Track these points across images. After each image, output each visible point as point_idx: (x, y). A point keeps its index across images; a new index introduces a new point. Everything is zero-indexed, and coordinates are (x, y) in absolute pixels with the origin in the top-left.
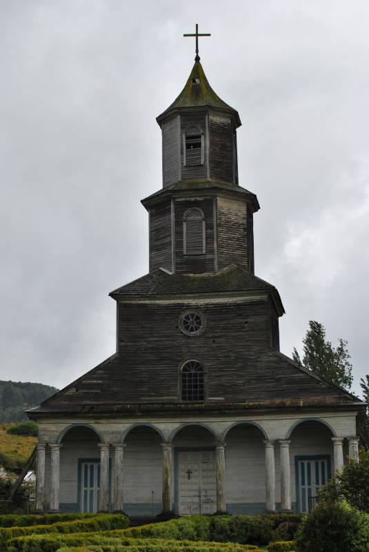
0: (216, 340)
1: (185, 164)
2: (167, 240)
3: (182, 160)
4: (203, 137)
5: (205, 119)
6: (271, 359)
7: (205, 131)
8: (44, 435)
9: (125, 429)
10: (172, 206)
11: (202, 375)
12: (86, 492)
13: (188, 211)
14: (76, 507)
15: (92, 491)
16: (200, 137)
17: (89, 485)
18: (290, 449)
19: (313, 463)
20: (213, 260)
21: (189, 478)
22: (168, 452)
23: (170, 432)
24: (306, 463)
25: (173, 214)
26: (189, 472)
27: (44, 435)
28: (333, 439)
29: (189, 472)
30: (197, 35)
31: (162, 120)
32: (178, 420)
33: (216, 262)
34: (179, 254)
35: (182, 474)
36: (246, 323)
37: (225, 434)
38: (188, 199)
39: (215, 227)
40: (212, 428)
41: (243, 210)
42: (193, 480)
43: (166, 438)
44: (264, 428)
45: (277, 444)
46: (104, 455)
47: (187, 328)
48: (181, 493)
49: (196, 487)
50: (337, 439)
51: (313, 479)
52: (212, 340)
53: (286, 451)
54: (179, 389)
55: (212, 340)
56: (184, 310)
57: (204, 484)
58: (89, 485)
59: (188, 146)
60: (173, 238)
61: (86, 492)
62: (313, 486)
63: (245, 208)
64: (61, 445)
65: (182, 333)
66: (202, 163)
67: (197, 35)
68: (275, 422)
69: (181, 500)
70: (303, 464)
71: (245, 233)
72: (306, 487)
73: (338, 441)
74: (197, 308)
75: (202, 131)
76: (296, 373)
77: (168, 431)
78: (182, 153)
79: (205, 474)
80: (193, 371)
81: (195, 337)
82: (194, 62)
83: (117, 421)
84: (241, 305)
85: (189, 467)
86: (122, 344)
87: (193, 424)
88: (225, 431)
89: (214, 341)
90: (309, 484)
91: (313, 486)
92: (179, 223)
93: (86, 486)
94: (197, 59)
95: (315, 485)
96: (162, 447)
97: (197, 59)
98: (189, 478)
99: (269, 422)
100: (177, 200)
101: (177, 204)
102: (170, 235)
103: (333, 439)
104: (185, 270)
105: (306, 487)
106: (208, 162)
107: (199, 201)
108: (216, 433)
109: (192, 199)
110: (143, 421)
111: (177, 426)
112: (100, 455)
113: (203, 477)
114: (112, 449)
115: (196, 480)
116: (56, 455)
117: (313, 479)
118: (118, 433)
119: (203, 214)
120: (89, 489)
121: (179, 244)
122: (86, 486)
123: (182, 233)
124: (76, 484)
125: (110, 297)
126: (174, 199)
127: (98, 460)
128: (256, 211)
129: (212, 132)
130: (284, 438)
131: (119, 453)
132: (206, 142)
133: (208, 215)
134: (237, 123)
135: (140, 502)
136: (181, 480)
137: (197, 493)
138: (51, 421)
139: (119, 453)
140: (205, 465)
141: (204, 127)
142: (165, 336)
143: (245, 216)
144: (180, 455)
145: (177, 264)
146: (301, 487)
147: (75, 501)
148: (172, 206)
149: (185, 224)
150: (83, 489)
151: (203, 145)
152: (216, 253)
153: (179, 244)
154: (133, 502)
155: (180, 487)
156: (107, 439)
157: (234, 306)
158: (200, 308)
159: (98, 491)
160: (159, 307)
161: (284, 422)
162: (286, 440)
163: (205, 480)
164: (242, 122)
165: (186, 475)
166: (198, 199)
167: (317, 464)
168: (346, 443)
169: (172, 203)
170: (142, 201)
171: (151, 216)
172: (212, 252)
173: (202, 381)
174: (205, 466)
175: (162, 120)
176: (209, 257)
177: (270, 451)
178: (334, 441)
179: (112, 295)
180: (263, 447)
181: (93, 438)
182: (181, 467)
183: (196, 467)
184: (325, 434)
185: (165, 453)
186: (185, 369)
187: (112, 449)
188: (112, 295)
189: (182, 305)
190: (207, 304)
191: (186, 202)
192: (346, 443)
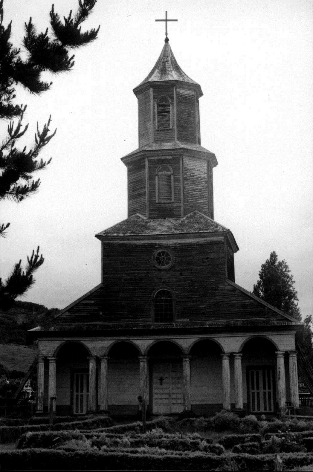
0: (182, 272)
1: (157, 129)
2: (142, 191)
3: (155, 125)
4: (171, 106)
5: (173, 91)
6: (226, 288)
7: (173, 101)
8: (43, 350)
9: (109, 345)
10: (147, 163)
11: (171, 301)
12: (77, 396)
13: (160, 167)
14: (70, 408)
15: (82, 396)
16: (169, 106)
17: (79, 390)
18: (242, 360)
20: (180, 207)
21: (161, 384)
22: (143, 365)
23: (146, 347)
25: (147, 170)
26: (161, 379)
27: (43, 350)
28: (276, 353)
29: (161, 379)
30: (166, 20)
31: (137, 91)
33: (182, 209)
34: (152, 203)
36: (207, 258)
37: (190, 348)
38: (159, 158)
39: (182, 180)
40: (179, 343)
41: (205, 167)
42: (164, 386)
43: (143, 352)
45: (232, 357)
46: (92, 365)
47: (159, 263)
48: (155, 396)
49: (167, 391)
50: (280, 353)
51: (261, 385)
52: (179, 273)
53: (238, 363)
54: (152, 314)
55: (179, 273)
56: (156, 248)
57: (173, 389)
58: (79, 390)
59: (159, 112)
60: (147, 190)
61: (77, 396)
62: (261, 391)
63: (207, 165)
65: (155, 267)
66: (171, 128)
67: (166, 20)
68: (230, 339)
69: (154, 402)
71: (206, 185)
72: (255, 391)
73: (281, 354)
74: (168, 247)
75: (170, 101)
76: (247, 299)
78: (154, 119)
79: (174, 381)
80: (164, 298)
81: (165, 270)
82: (164, 43)
84: (204, 245)
85: (162, 375)
86: (106, 276)
87: (164, 340)
88: (190, 346)
89: (181, 274)
90: (258, 389)
91: (261, 391)
92: (151, 177)
93: (77, 391)
94: (167, 40)
95: (262, 389)
96: (139, 358)
97: (167, 40)
99: (227, 340)
100: (151, 158)
101: (150, 162)
102: (144, 187)
103: (276, 353)
104: (156, 216)
105: (255, 391)
106: (175, 127)
107: (169, 160)
108: (183, 347)
109: (163, 158)
110: (123, 338)
111: (151, 342)
112: (89, 366)
113: (173, 383)
114: (98, 361)
115: (166, 386)
116: (52, 367)
117: (261, 385)
118: (103, 347)
119: (171, 170)
120: (80, 393)
121: (152, 195)
122: (77, 391)
123: (154, 185)
124: (69, 390)
125: (96, 238)
126: (148, 157)
127: (88, 370)
128: (215, 166)
129: (179, 103)
130: (237, 351)
131: (104, 365)
132: (173, 110)
133: (176, 171)
134: (200, 94)
135: (121, 404)
136: (154, 386)
137: (167, 396)
138: (49, 339)
139: (104, 365)
141: (172, 98)
142: (141, 270)
143: (206, 171)
145: (150, 210)
146: (251, 391)
147: (68, 403)
148: (147, 163)
149: (157, 177)
150: (75, 394)
151: (171, 113)
152: (182, 201)
153: (152, 195)
154: (116, 404)
155: (155, 391)
156: (94, 353)
157: (197, 245)
158: (170, 247)
159: (88, 396)
160: (136, 246)
161: (238, 338)
162: (239, 353)
163: (174, 386)
164: (203, 94)
165: (159, 381)
166: (168, 157)
168: (287, 356)
169: (146, 160)
170: (122, 159)
171: (129, 171)
172: (179, 200)
173: (171, 305)
174: (174, 374)
175: (137, 91)
176: (175, 205)
177: (226, 363)
178: (278, 354)
179: (97, 236)
180: (221, 359)
181: (85, 353)
182: (155, 375)
183: (167, 375)
184: (272, 348)
185: (142, 364)
186: (157, 297)
187: (98, 361)
188: (97, 236)
189: (155, 245)
190: (176, 244)
191: (158, 160)
192: (287, 356)
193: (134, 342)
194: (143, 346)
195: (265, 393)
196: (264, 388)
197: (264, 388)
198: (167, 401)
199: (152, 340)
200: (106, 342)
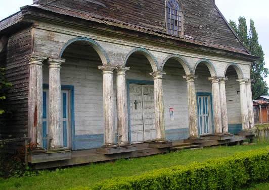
8: (42, 45)
19: (202, 98)
21: (136, 109)
23: (162, 61)
24: (202, 98)
26: (136, 103)
29: (136, 103)
32: (168, 51)
35: (132, 104)
44: (215, 67)
57: (146, 113)
64: (63, 61)
70: (200, 99)
77: (160, 60)
83: (122, 41)
98: (136, 109)
114: (115, 73)
118: (121, 55)
131: (121, 79)
140: (146, 97)
144: (131, 85)
154: (96, 133)
167: (203, 98)
183: (140, 98)
193: (152, 54)
194: (159, 60)
195: (204, 117)
196: (204, 113)
197: (204, 113)
198: (140, 128)
199: (167, 54)
200: (124, 48)
